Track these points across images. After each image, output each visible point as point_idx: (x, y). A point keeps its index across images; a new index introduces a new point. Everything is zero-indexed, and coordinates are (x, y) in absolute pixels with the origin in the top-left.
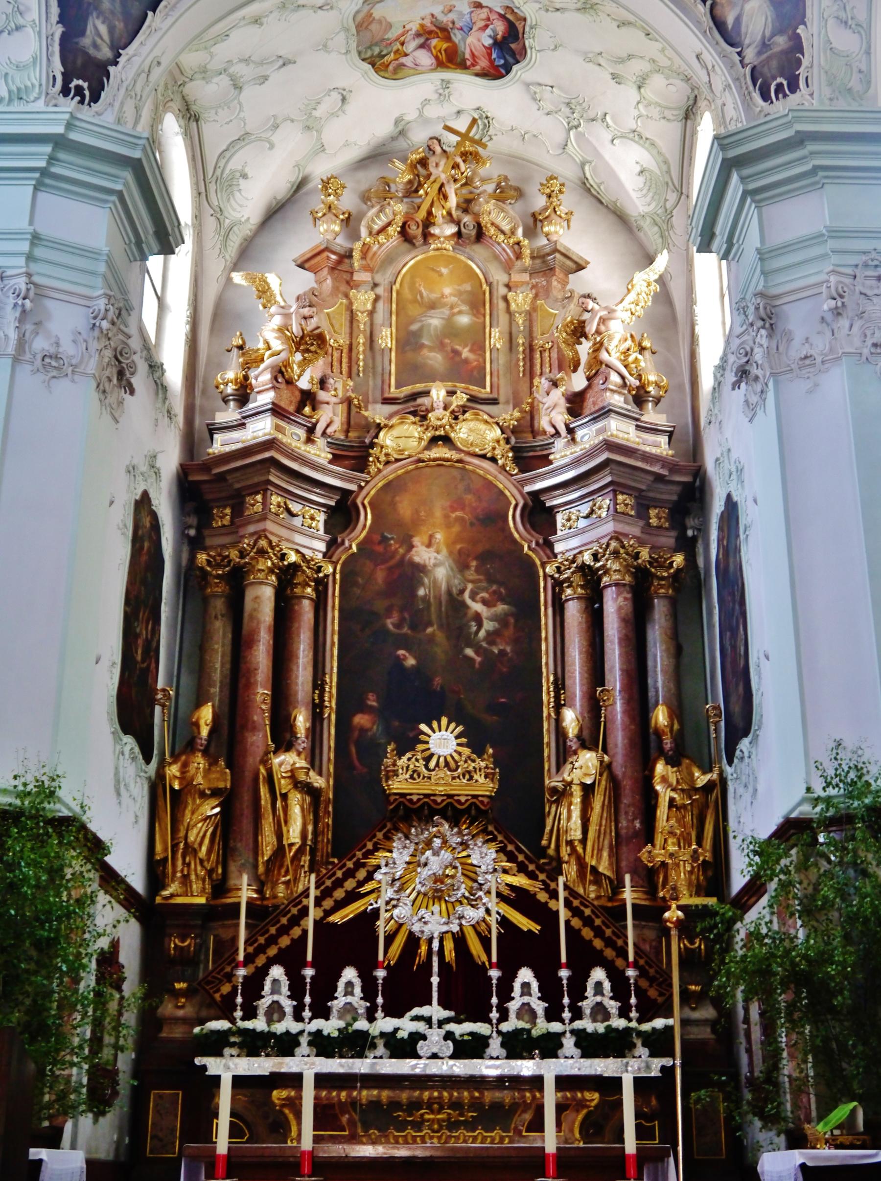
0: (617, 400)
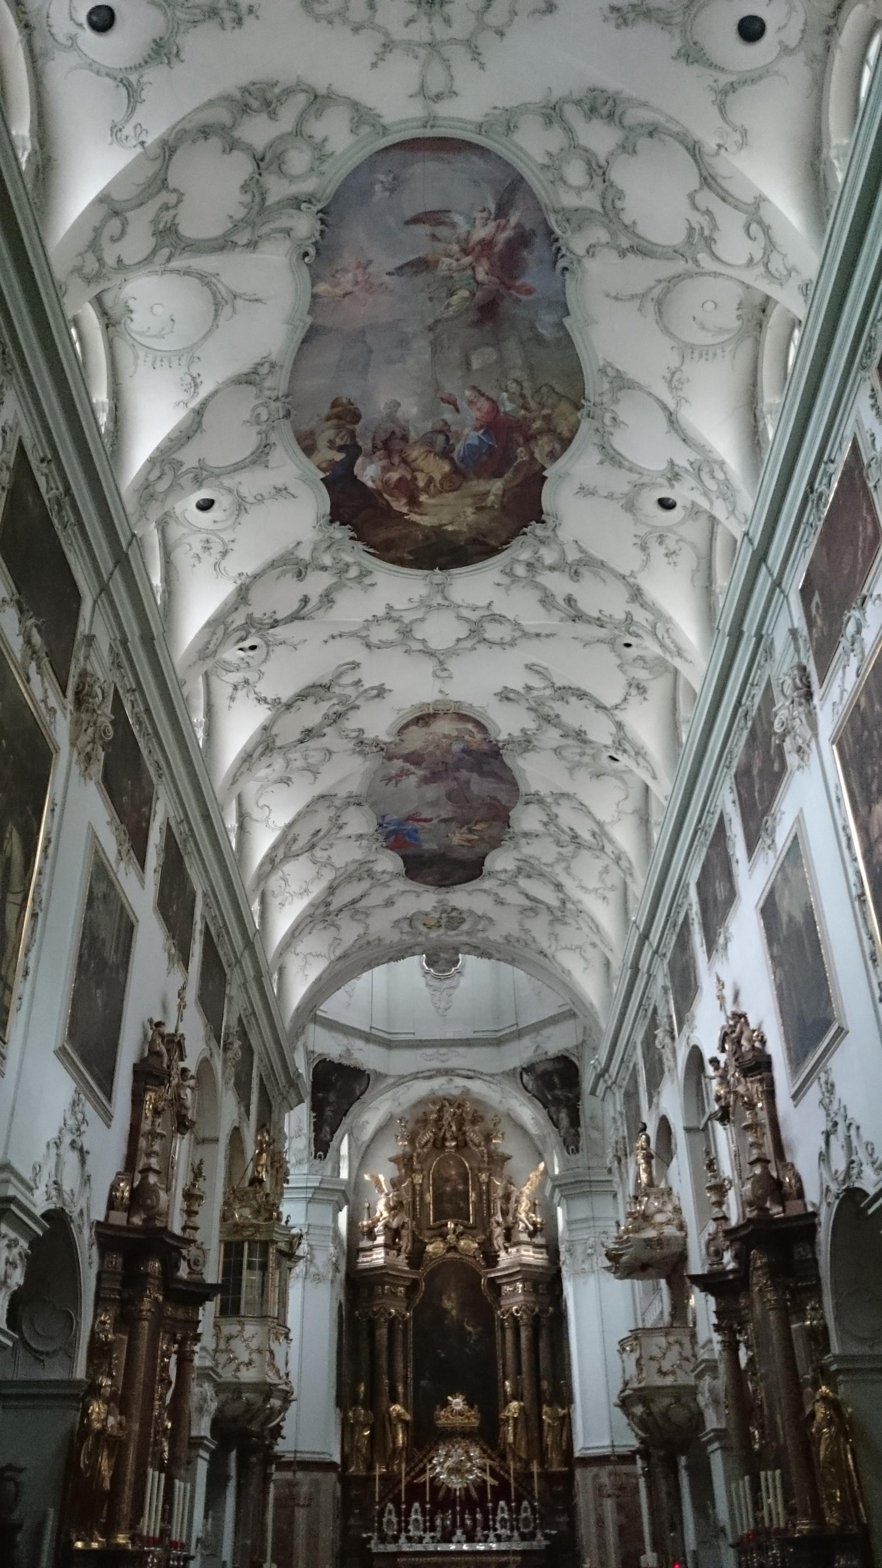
0: (524, 1237)
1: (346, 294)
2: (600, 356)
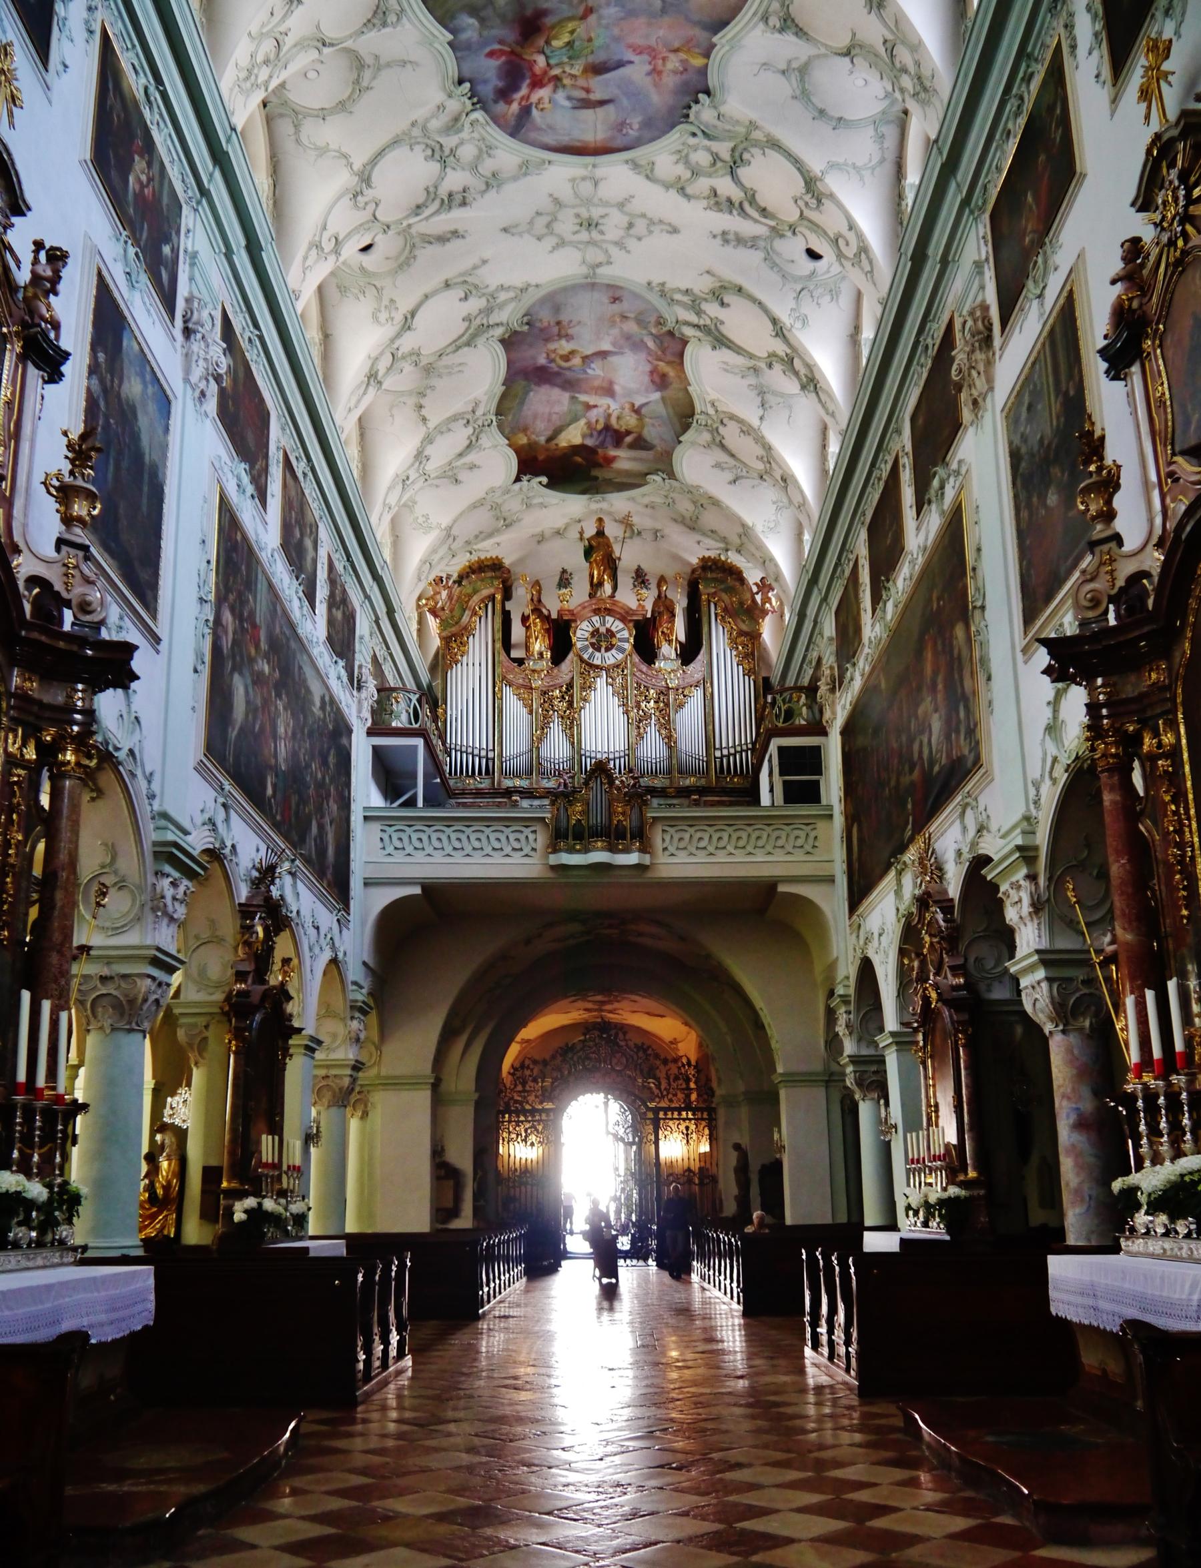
1: (676, 51)
2: (408, 25)
